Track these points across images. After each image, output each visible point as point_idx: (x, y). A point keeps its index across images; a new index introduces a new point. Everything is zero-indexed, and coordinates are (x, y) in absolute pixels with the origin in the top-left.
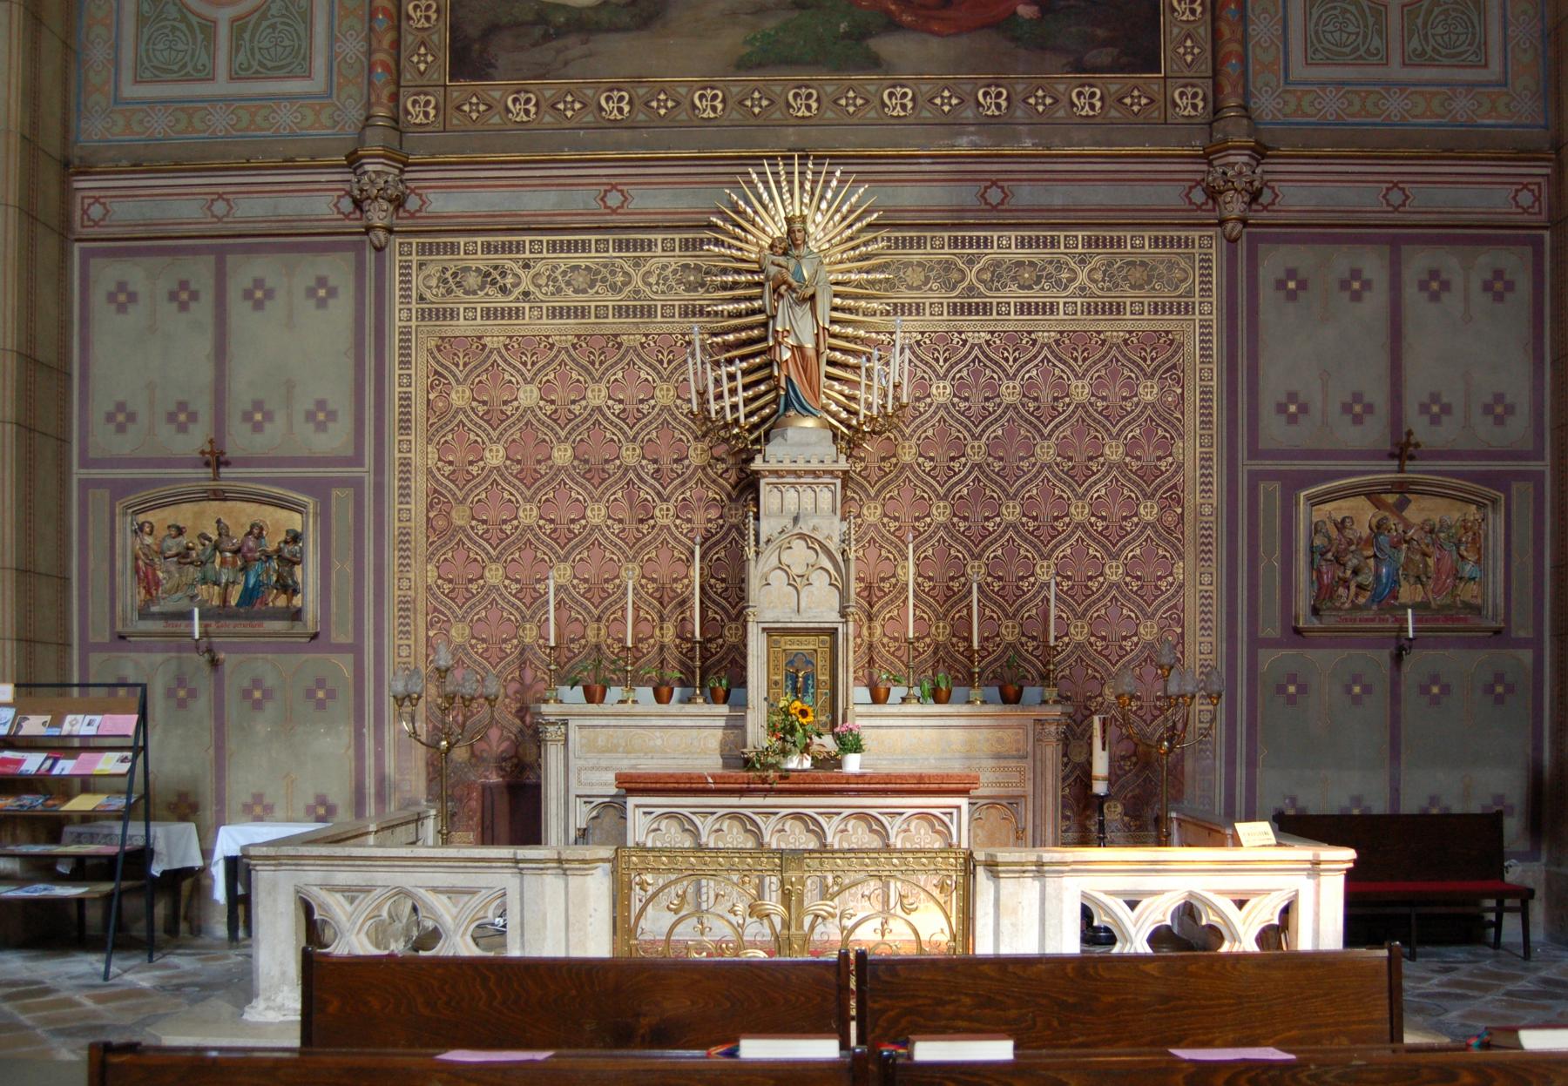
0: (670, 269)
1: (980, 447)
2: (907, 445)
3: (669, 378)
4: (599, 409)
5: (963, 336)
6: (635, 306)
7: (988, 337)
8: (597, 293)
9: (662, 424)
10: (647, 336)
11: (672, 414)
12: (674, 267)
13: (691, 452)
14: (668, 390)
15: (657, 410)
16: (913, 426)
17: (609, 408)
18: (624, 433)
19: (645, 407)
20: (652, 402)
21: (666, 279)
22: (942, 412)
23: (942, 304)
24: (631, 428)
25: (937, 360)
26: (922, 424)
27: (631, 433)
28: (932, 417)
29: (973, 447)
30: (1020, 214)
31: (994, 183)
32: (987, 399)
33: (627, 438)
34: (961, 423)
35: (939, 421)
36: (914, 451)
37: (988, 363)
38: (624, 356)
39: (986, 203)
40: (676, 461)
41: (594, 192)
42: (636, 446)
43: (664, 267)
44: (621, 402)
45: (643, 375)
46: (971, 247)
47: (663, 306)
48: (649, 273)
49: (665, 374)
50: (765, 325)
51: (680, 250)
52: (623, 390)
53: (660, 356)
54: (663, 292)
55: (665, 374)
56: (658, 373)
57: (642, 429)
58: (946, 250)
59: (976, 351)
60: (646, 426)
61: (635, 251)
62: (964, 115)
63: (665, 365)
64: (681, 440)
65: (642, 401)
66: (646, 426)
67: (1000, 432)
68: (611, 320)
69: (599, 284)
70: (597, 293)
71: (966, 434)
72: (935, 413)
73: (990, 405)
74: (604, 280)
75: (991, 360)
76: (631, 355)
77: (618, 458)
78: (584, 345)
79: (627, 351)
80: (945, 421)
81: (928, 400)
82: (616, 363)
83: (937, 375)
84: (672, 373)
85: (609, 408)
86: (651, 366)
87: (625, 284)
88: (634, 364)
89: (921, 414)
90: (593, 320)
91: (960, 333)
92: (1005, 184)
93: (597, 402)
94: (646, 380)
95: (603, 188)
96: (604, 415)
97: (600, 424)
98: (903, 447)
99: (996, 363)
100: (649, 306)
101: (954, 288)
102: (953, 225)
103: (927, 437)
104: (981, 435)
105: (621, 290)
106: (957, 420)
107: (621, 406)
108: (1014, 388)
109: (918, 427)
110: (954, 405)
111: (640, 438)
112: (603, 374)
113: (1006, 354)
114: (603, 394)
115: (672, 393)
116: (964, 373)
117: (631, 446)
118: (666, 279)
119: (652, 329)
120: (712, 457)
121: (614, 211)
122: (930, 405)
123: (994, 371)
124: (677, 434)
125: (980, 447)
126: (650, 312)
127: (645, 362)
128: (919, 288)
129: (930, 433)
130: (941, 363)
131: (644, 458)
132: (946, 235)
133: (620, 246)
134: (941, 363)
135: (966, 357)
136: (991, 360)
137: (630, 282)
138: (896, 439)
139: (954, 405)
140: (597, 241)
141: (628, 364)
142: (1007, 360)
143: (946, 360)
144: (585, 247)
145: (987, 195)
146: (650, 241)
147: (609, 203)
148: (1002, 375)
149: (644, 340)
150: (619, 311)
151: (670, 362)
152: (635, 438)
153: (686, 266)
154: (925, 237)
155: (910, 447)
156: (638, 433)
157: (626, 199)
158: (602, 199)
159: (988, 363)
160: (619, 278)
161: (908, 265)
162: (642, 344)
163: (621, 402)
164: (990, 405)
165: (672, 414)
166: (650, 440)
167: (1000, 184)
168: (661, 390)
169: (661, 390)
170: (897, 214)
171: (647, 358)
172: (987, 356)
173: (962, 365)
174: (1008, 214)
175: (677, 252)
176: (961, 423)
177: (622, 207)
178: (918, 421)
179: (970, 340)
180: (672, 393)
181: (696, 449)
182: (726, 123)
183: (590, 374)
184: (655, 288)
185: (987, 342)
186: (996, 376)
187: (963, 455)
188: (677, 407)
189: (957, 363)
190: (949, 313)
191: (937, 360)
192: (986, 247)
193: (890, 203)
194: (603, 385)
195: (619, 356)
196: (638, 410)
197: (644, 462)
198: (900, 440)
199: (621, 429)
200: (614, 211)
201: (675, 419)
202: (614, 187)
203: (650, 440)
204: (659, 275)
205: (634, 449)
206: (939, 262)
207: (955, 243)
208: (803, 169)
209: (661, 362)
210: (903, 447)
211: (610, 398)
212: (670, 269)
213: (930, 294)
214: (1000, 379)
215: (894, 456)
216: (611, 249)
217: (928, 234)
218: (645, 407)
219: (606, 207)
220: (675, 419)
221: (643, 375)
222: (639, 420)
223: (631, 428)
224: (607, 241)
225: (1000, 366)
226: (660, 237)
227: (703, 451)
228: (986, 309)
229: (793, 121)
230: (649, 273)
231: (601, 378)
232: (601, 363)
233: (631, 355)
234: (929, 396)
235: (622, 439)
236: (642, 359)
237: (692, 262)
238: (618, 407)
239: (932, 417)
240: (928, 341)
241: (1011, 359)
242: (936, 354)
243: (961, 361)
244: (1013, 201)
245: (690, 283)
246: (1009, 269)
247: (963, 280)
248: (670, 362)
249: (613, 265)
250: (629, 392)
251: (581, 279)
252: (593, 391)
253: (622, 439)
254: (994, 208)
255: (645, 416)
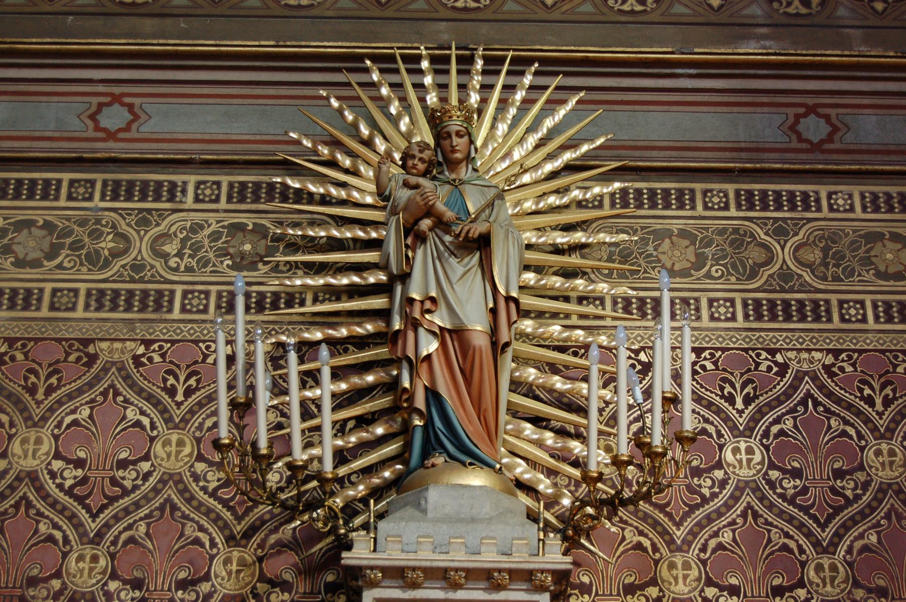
0: (207, 232)
1: (834, 568)
2: (679, 560)
3: (184, 420)
4: (33, 477)
5: (779, 358)
6: (131, 293)
7: (829, 360)
8: (60, 267)
9: (162, 508)
10: (147, 343)
11: (184, 491)
12: (214, 227)
13: (217, 567)
14: (181, 443)
15: (152, 481)
16: (689, 523)
17: (53, 475)
18: (78, 526)
19: (128, 477)
20: (145, 466)
21: (196, 248)
22: (747, 498)
23: (732, 301)
24: (94, 516)
25: (731, 400)
26: (709, 519)
27: (92, 526)
28: (728, 507)
29: (819, 568)
30: (866, 157)
31: (811, 110)
32: (839, 474)
33: (82, 535)
34: (791, 520)
35: (744, 515)
36: (694, 573)
37: (834, 408)
38: (97, 379)
39: (800, 139)
40: (183, 585)
41: (78, 105)
42: (101, 551)
43: (196, 228)
44: (79, 463)
45: (132, 414)
46: (779, 208)
47: (185, 294)
48: (165, 236)
49: (177, 414)
50: (391, 338)
51: (229, 199)
52: (87, 443)
53: (171, 381)
54: (189, 269)
55: (177, 414)
56: (164, 411)
57: (117, 518)
58: (733, 212)
59: (807, 385)
60: (127, 511)
61: (143, 199)
62: (746, 12)
63: (180, 397)
64: (197, 542)
65: (123, 464)
66: (127, 511)
67: (874, 539)
68: (80, 313)
69: (64, 252)
70: (60, 267)
71: (803, 541)
72: (735, 498)
73: (848, 487)
74: (76, 246)
75: (839, 401)
76: (113, 377)
77: (58, 575)
78: (20, 356)
79: (105, 370)
80: (756, 515)
81: (719, 474)
82: (80, 391)
83: (733, 428)
84: (192, 412)
85: (53, 475)
86: (150, 398)
87: (116, 254)
88: (117, 393)
89: (705, 500)
90: (45, 312)
91: (772, 352)
92: (833, 112)
93: (30, 463)
94: (138, 424)
95: (95, 100)
96: (40, 489)
97: (29, 505)
98: (672, 566)
99: (849, 407)
100: (160, 293)
101: (753, 275)
102: (743, 171)
103: (720, 546)
104: (834, 544)
105: (107, 264)
106: (781, 514)
107: (79, 473)
108: (892, 453)
109: (700, 526)
110: (772, 484)
111: (109, 537)
112: (51, 410)
113: (867, 391)
114: (45, 448)
115: (187, 450)
116: (789, 424)
117: (88, 552)
118: (196, 248)
119: (159, 332)
120: (262, 578)
121: (111, 136)
122: (723, 483)
123: (846, 422)
124: (190, 530)
125: (834, 568)
126: (162, 302)
127: (140, 392)
128: (684, 273)
129: (726, 537)
130: (739, 404)
131: (114, 576)
132: (731, 188)
133: (115, 191)
134: (739, 404)
135: (788, 395)
136: (839, 401)
137: (125, 251)
138: (655, 549)
139: (772, 484)
140: (72, 182)
141: (105, 394)
142: (870, 401)
143: (747, 401)
144: (48, 191)
145: (800, 128)
146: (173, 185)
147: (104, 122)
148: (864, 430)
149: (141, 350)
150: (98, 299)
151: (188, 393)
152: (100, 535)
153: (239, 228)
154: (692, 191)
155: (687, 566)
156: (107, 526)
157: (136, 117)
158: (92, 117)
159: (834, 408)
160: (107, 244)
161: (661, 235)
162: (136, 359)
163: (79, 463)
164: (848, 487)
165: (184, 491)
166: (132, 540)
167: (822, 111)
168: (166, 443)
169: (166, 443)
170: (637, 153)
171: (144, 384)
172: (830, 395)
173: (782, 409)
174: (842, 157)
175: (223, 204)
176: (791, 520)
177: (127, 129)
178: (699, 514)
179: (794, 366)
180: (187, 450)
181: (228, 561)
182: (330, 13)
183: (24, 409)
184: (173, 263)
185: (827, 368)
186: (852, 432)
187: (801, 584)
188: (196, 478)
189: (770, 406)
190: (746, 317)
191: (731, 400)
192: (807, 208)
193: (625, 136)
194: (46, 433)
195: (87, 378)
196: (114, 482)
197: (113, 586)
198: (664, 550)
199: (72, 517)
200: (111, 136)
201: (190, 500)
202: (117, 99)
203: (132, 540)
204: (184, 241)
205: (95, 559)
206: (722, 232)
207: (748, 201)
208: (464, 79)
209: (172, 392)
210: (672, 566)
211: (58, 456)
212: (207, 232)
213: (709, 284)
214: (860, 436)
215: (653, 582)
216: (97, 195)
217: (698, 187)
218: (128, 477)
219: (97, 128)
220: (190, 500)
221: (132, 414)
222: (112, 500)
223: (94, 516)
224: (92, 183)
225: (859, 413)
226: (192, 179)
227: (242, 563)
228: (819, 311)
229: (444, 14)
230: (165, 236)
231: (44, 419)
232: (49, 390)
233: (113, 377)
234: (719, 465)
235: (72, 536)
236: (133, 385)
237: (249, 221)
238: (71, 475)
239: (728, 507)
240: (709, 366)
241: (879, 401)
242: (728, 389)
243: (779, 401)
244: (849, 138)
245: (243, 255)
246: (854, 246)
247: (769, 261)
248: (188, 393)
249: (98, 221)
250: (98, 447)
251: (32, 244)
252: (24, 441)
253: (72, 536)
254: (816, 147)
255: (126, 492)
